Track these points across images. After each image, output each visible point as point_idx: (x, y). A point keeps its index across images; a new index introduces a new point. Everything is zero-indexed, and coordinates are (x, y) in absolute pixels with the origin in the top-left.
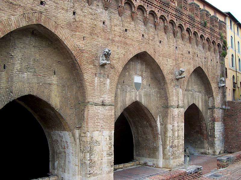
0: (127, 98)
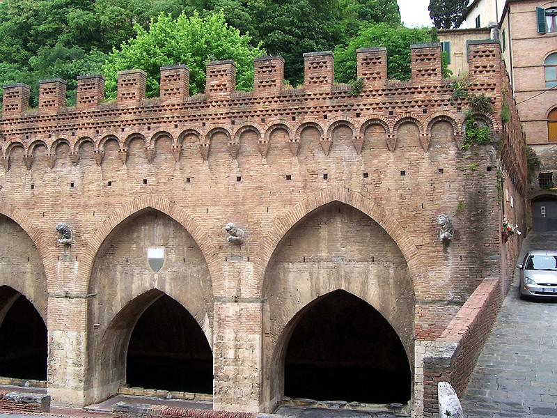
0: (134, 286)
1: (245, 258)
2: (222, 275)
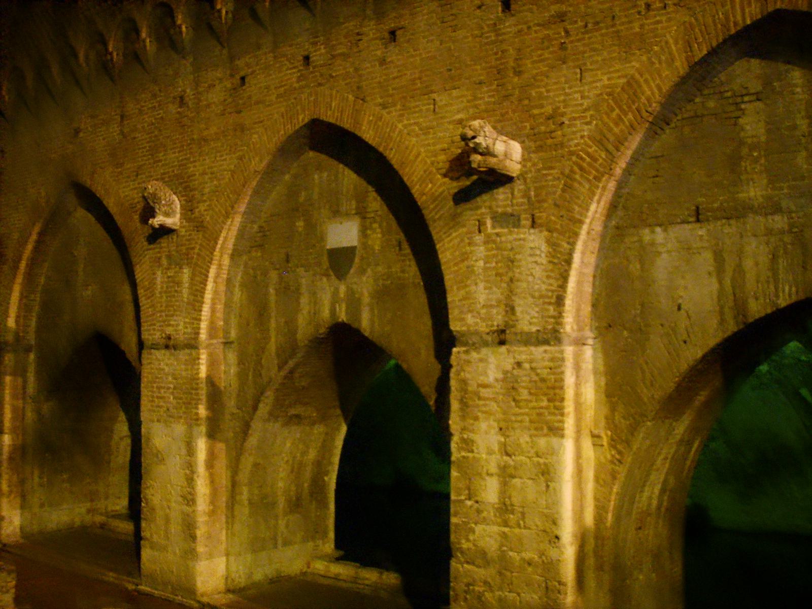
1: (526, 222)
2: (470, 270)
